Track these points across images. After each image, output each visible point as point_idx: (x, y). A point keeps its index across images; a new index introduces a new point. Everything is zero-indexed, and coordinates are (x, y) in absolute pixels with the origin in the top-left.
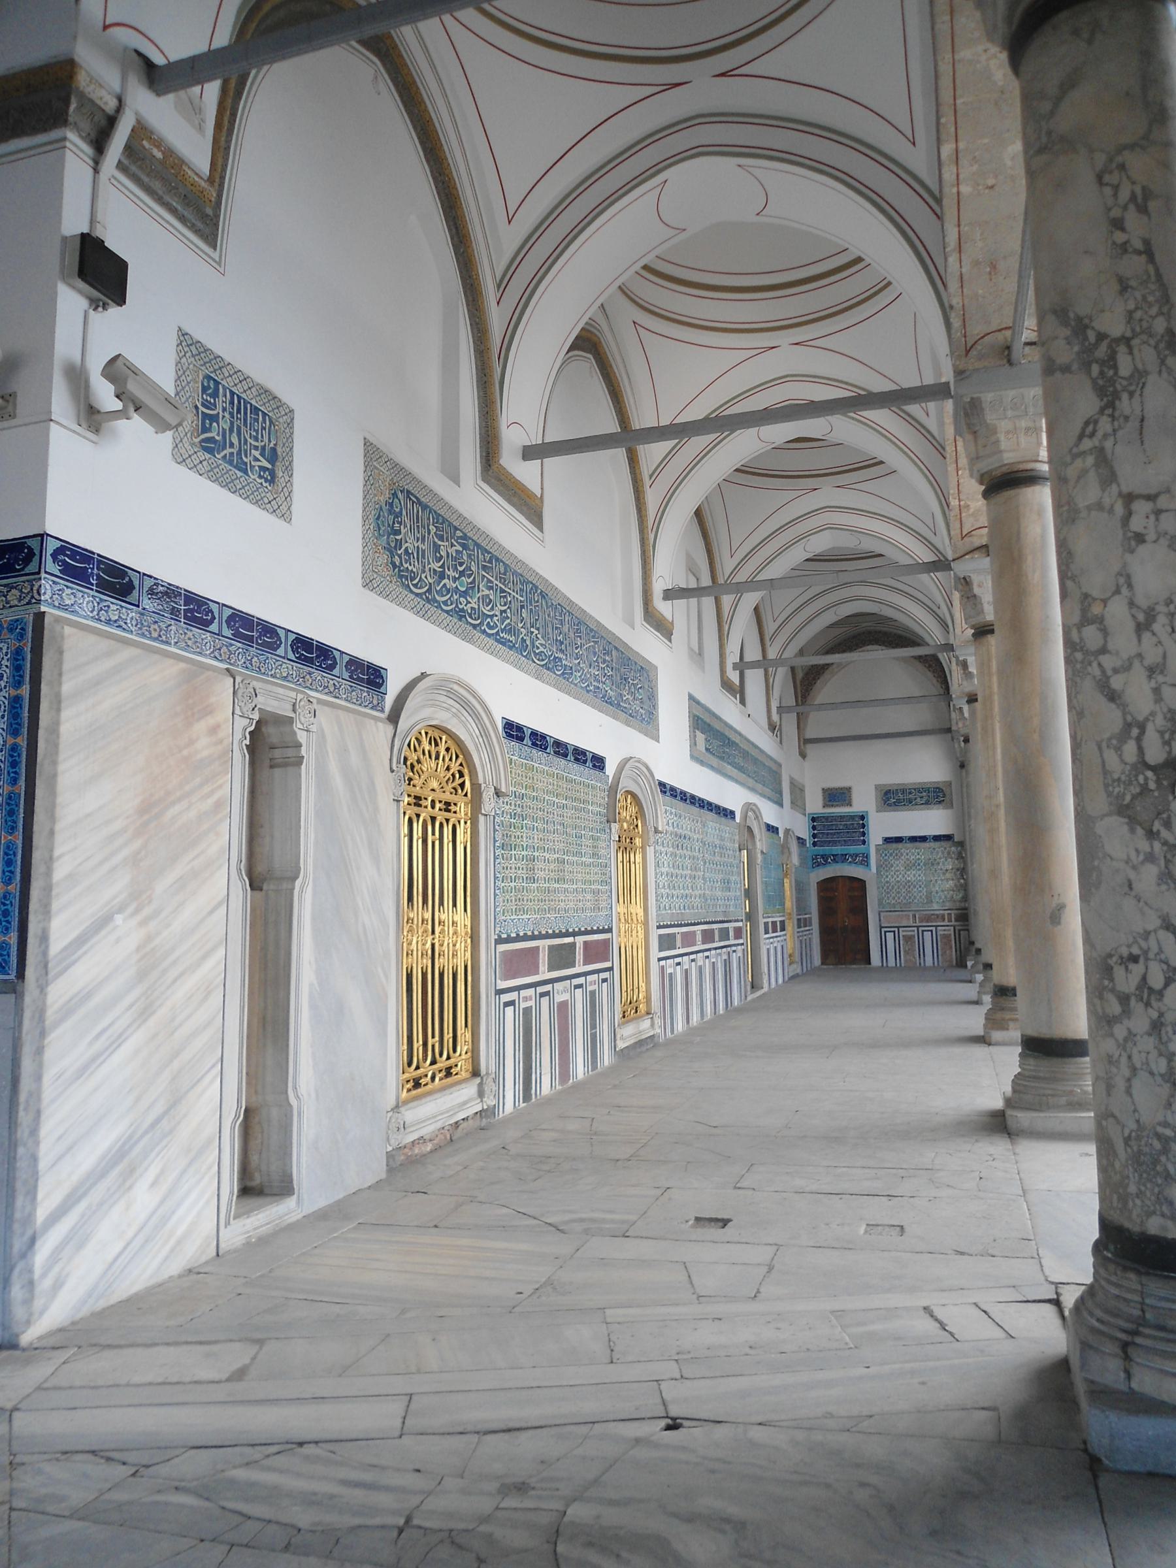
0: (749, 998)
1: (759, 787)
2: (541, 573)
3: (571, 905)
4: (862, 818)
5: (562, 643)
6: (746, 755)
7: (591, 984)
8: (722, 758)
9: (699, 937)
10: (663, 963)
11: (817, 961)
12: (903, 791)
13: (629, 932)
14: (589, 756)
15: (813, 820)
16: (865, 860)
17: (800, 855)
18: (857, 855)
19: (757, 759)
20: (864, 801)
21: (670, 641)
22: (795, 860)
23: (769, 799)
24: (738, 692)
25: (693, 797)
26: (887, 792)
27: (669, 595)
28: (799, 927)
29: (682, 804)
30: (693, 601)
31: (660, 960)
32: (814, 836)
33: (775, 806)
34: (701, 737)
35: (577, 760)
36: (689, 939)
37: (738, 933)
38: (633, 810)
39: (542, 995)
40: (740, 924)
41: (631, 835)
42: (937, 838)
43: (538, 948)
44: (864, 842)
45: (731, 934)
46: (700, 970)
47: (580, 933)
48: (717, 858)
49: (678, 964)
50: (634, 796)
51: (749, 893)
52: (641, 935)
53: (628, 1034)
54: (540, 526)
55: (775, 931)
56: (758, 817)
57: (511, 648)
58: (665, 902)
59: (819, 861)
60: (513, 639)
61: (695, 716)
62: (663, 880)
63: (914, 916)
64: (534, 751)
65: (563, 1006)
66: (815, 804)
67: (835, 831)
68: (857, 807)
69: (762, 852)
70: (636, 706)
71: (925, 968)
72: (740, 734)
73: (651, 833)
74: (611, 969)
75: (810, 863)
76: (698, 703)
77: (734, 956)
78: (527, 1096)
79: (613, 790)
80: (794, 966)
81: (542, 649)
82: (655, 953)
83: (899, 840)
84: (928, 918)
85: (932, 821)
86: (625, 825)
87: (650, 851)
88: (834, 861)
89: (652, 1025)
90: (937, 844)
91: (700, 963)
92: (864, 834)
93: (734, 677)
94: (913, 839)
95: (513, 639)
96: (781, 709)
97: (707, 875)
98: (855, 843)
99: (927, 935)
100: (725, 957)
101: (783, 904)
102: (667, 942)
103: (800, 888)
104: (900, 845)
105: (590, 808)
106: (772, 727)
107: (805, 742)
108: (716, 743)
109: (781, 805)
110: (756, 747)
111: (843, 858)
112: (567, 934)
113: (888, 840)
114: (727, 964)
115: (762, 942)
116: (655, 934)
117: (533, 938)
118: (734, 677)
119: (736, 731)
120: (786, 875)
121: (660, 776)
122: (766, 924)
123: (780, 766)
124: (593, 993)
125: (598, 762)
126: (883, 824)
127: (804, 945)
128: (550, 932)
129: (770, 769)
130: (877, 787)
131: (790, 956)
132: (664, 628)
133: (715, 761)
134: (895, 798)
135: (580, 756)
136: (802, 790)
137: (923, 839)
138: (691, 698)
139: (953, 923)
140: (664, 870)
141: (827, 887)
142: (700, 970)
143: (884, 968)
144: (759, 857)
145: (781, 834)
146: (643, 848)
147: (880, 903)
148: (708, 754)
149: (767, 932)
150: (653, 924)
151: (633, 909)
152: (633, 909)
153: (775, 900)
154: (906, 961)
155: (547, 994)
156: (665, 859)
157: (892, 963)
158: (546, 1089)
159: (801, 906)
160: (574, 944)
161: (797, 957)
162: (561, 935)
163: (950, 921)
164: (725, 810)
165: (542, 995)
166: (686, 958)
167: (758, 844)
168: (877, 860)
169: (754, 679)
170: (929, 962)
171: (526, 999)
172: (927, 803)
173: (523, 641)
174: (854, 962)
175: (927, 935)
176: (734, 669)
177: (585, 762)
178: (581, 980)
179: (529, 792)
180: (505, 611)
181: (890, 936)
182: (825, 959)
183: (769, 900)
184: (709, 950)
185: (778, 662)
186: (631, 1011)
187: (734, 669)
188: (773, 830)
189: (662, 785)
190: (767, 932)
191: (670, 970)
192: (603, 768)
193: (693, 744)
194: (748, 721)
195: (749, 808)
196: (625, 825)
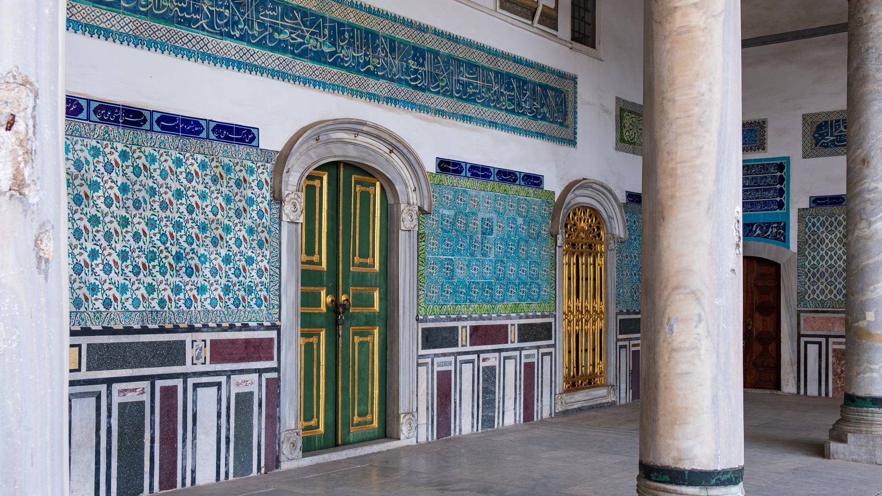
4: (781, 167)
18: (769, 225)
26: (819, 127)
44: (781, 205)
92: (781, 192)
113: (818, 201)
130: (805, 117)
143: (801, 396)
154: (835, 389)
157: (813, 390)
168: (799, 232)
181: (813, 350)
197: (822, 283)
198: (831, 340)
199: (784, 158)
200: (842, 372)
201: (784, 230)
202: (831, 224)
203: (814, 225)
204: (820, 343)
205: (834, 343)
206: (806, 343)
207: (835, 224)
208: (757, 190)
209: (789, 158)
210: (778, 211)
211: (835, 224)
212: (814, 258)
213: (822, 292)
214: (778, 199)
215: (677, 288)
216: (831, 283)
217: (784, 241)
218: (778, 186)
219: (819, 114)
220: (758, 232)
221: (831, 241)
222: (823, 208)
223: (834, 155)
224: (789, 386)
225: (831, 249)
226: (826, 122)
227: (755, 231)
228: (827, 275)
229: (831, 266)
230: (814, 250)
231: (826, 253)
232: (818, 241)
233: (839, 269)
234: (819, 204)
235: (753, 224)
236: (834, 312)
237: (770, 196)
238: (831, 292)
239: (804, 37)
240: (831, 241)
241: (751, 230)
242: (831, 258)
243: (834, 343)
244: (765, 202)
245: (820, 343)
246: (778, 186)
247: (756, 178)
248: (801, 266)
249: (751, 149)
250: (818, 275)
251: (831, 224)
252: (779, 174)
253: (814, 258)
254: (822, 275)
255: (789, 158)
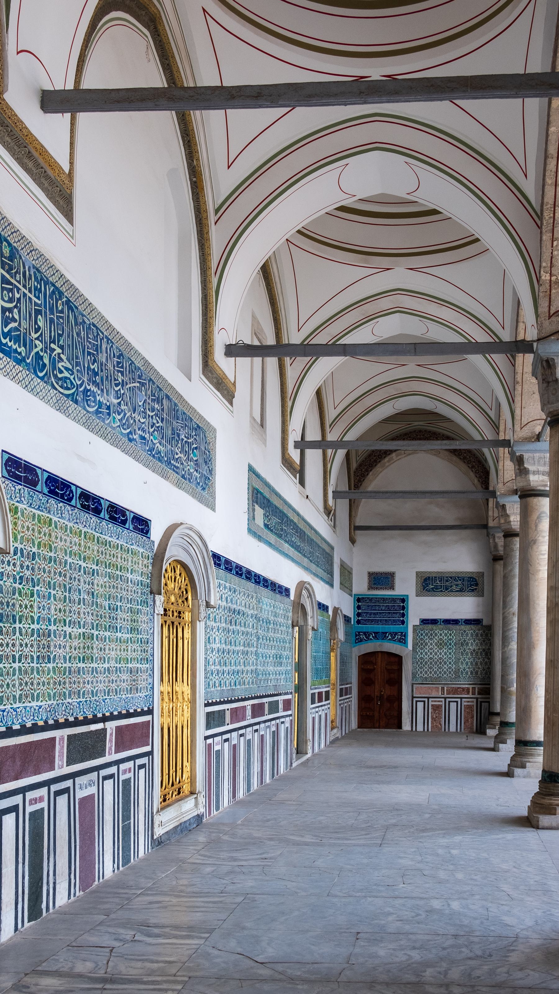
0: (294, 765)
1: (313, 567)
2: (68, 276)
3: (101, 686)
4: (403, 601)
5: (96, 374)
6: (302, 534)
7: (125, 772)
8: (280, 536)
9: (249, 712)
10: (210, 741)
11: (354, 724)
12: (441, 579)
13: (172, 712)
14: (130, 516)
15: (359, 600)
16: (403, 640)
17: (347, 634)
18: (396, 634)
19: (312, 540)
20: (405, 586)
21: (231, 404)
22: (341, 635)
23: (321, 579)
24: (299, 472)
25: (249, 572)
26: (426, 580)
27: (232, 350)
28: (341, 695)
29: (237, 579)
30: (258, 360)
31: (206, 738)
32: (359, 615)
33: (327, 586)
34: (259, 512)
35: (113, 519)
36: (237, 714)
37: (287, 705)
38: (183, 581)
39: (58, 793)
40: (289, 697)
41: (180, 608)
42: (468, 622)
43: (54, 739)
44: (403, 622)
45: (281, 706)
46: (249, 743)
47: (112, 718)
48: (271, 634)
49: (226, 740)
50: (184, 566)
51: (300, 668)
52: (187, 715)
53: (167, 820)
54: (68, 214)
55: (320, 700)
56: (311, 595)
57: (19, 362)
58: (215, 679)
59: (359, 638)
60: (22, 349)
61: (254, 489)
62: (213, 657)
63: (443, 689)
64: (52, 501)
65: (87, 801)
66: (360, 586)
67: (378, 610)
68: (399, 590)
69: (313, 629)
70: (190, 467)
71: (450, 734)
72: (298, 514)
73: (202, 608)
74: (150, 754)
75: (354, 639)
76: (258, 476)
77: (282, 728)
78: (35, 912)
79: (158, 558)
80: (335, 731)
81: (66, 374)
82: (201, 731)
83: (434, 622)
84: (455, 691)
85: (464, 606)
86: (173, 599)
87: (200, 627)
88: (376, 637)
89: (196, 805)
90: (468, 627)
91: (249, 737)
93: (295, 455)
94: (447, 622)
95: (22, 349)
96: (336, 494)
97: (260, 650)
98: (394, 622)
99: (453, 705)
100: (274, 729)
101: (328, 676)
102: (213, 720)
103: (343, 662)
104: (434, 627)
105: (130, 576)
106: (328, 511)
107: (355, 530)
108: (275, 520)
109: (332, 585)
110: (312, 528)
111: (383, 636)
112: (95, 720)
113: (424, 622)
114: (275, 735)
115: (309, 711)
116: (201, 713)
117: (46, 727)
118: (295, 455)
119: (294, 510)
120: (332, 650)
121: (215, 547)
122: (313, 695)
123: (332, 548)
124: (127, 782)
125: (142, 525)
126: (421, 608)
127: (344, 711)
128: (71, 719)
129: (324, 550)
131: (332, 722)
132: (225, 388)
133: (272, 538)
134: (431, 584)
135: (117, 514)
136: (350, 573)
137: (456, 622)
138: (251, 469)
139: (476, 696)
140: (216, 646)
141: (367, 662)
142: (249, 743)
143: (413, 732)
144: (310, 633)
145: (330, 612)
146: (193, 623)
147: (414, 675)
148: (266, 531)
149: (313, 702)
150: (200, 701)
151: (178, 688)
152: (178, 688)
153: (322, 672)
155: (66, 791)
156: (217, 635)
157: (420, 728)
158: (62, 899)
159: (343, 677)
160: (104, 730)
161: (338, 723)
162: (86, 722)
163: (473, 693)
164: (280, 587)
165: (58, 793)
166: (235, 734)
167: (310, 621)
169: (314, 458)
170: (453, 728)
171: (34, 801)
172: (461, 590)
173: (38, 357)
174: (387, 726)
175: (453, 705)
176: (296, 447)
177: (124, 522)
178: (113, 770)
179: (44, 552)
180: (10, 310)
181: (420, 705)
182: (360, 726)
183: (317, 672)
184: (259, 723)
185: (336, 445)
186: (174, 793)
187: (296, 447)
188: (323, 607)
189: (216, 557)
190: (313, 702)
191: (217, 748)
192: (148, 532)
193: (252, 518)
194: (306, 502)
195: (301, 586)
196: (173, 599)
197: (426, 668)
198: (430, 700)
199: (405, 595)
200: (436, 717)
201: (405, 637)
202: (431, 635)
203: (422, 635)
204: (424, 702)
205: (432, 701)
206: (417, 702)
207: (434, 635)
208: (389, 613)
209: (408, 596)
210: (401, 626)
211: (434, 635)
212: (421, 654)
213: (426, 673)
214: (402, 619)
215: (539, 674)
216: (431, 668)
217: (405, 643)
218: (402, 612)
219: (425, 572)
220: (390, 637)
221: (431, 644)
222: (427, 625)
223: (433, 596)
224: (406, 726)
225: (431, 649)
226: (429, 577)
227: (388, 637)
228: (429, 663)
229: (431, 658)
230: (422, 649)
231: (428, 651)
232: (424, 644)
233: (435, 660)
234: (425, 623)
235: (386, 633)
236: (432, 684)
237: (397, 617)
238: (431, 673)
239: (423, 529)
240: (431, 644)
241: (385, 636)
242: (431, 654)
243: (432, 701)
244: (394, 620)
245: (424, 702)
246: (402, 612)
247: (388, 606)
248: (414, 658)
249: (386, 589)
250: (424, 663)
251: (431, 635)
252: (402, 604)
253: (421, 654)
254: (426, 663)
255: (408, 596)
